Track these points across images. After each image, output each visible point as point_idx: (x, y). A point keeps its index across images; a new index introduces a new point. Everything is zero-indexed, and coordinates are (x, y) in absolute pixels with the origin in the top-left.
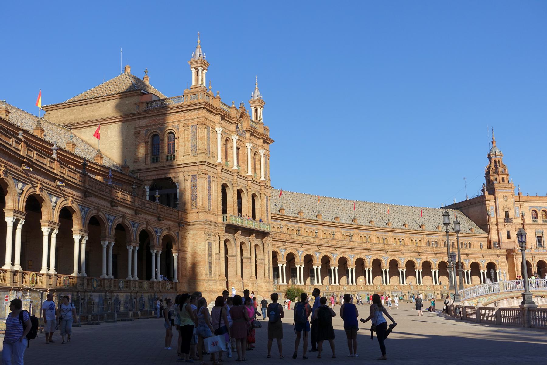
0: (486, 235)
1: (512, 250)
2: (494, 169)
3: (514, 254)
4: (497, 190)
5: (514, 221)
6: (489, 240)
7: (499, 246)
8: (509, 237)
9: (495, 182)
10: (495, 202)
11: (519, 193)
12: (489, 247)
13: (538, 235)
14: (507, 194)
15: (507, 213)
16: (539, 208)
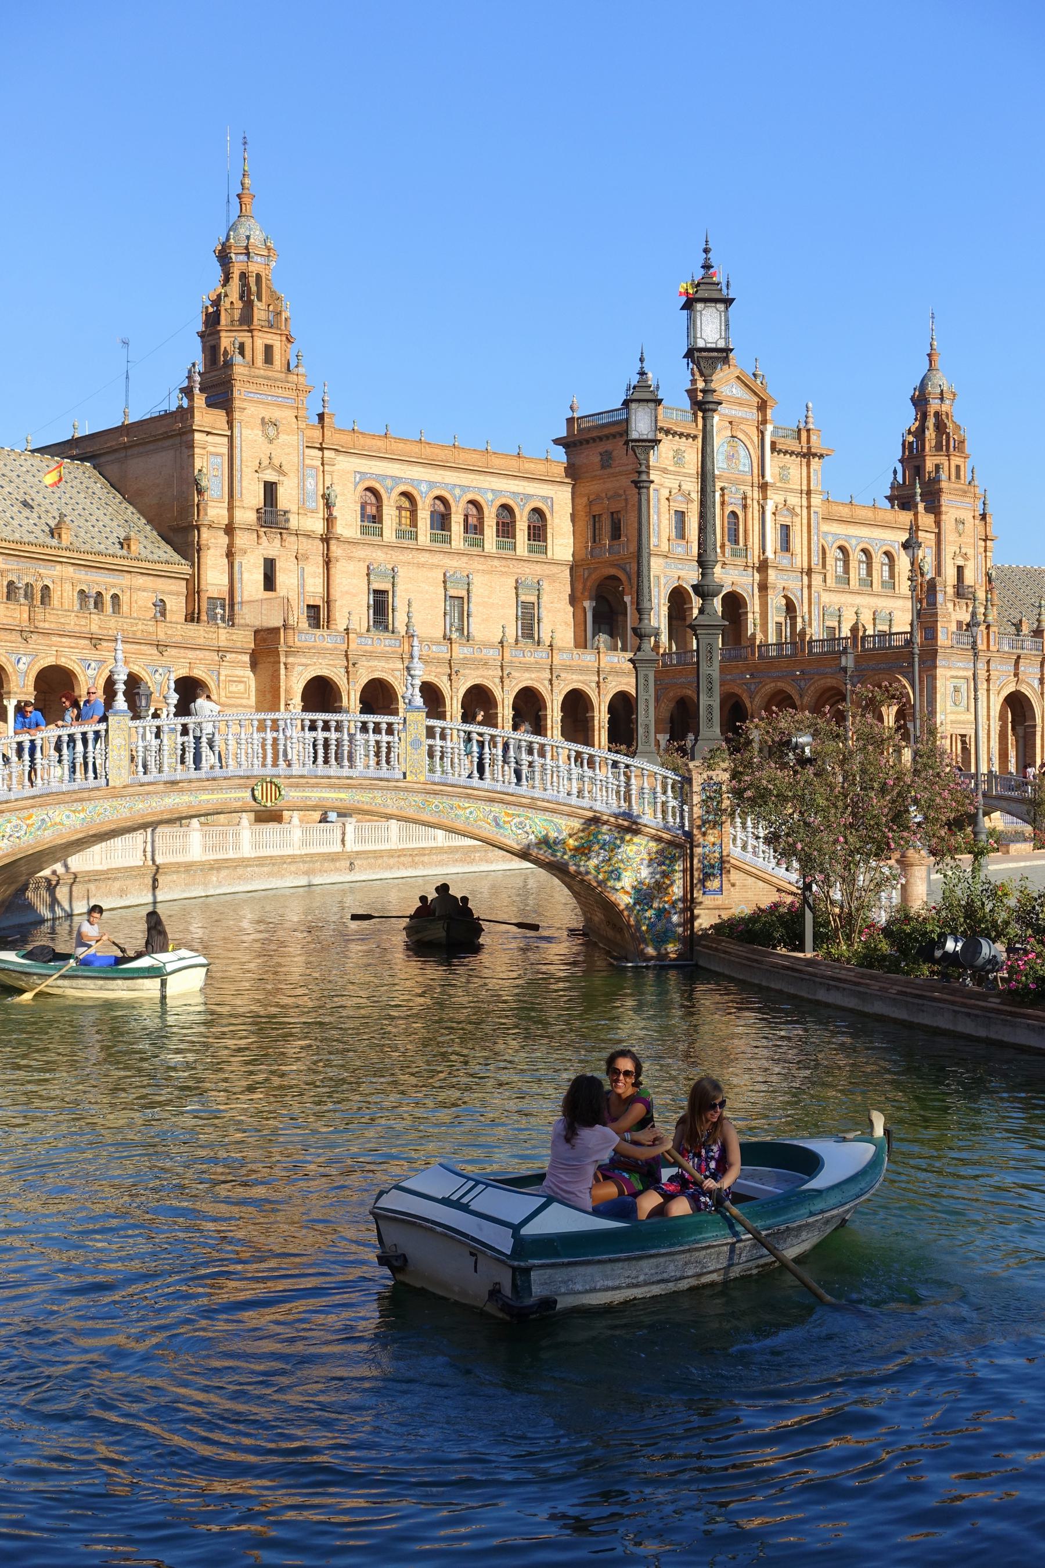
0: (185, 568)
1: (276, 630)
2: (239, 305)
3: (282, 648)
4: (240, 392)
5: (293, 524)
6: (194, 591)
7: (232, 618)
8: (269, 583)
9: (238, 359)
10: (231, 438)
11: (321, 417)
12: (192, 617)
13: (376, 586)
14: (276, 414)
15: (270, 489)
16: (389, 483)
